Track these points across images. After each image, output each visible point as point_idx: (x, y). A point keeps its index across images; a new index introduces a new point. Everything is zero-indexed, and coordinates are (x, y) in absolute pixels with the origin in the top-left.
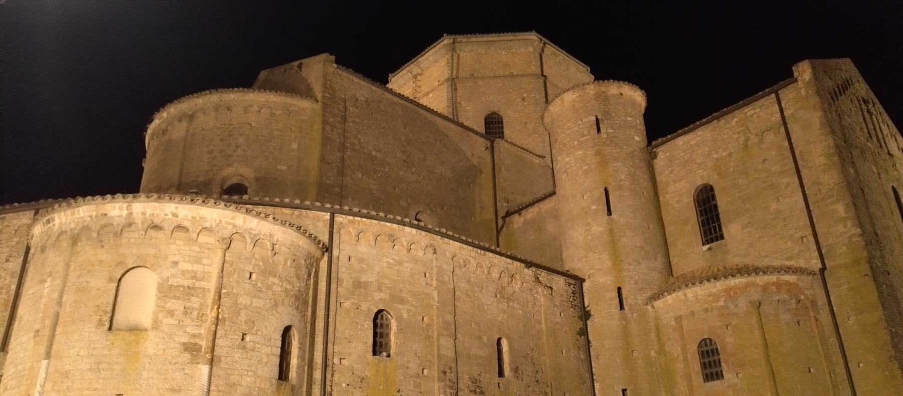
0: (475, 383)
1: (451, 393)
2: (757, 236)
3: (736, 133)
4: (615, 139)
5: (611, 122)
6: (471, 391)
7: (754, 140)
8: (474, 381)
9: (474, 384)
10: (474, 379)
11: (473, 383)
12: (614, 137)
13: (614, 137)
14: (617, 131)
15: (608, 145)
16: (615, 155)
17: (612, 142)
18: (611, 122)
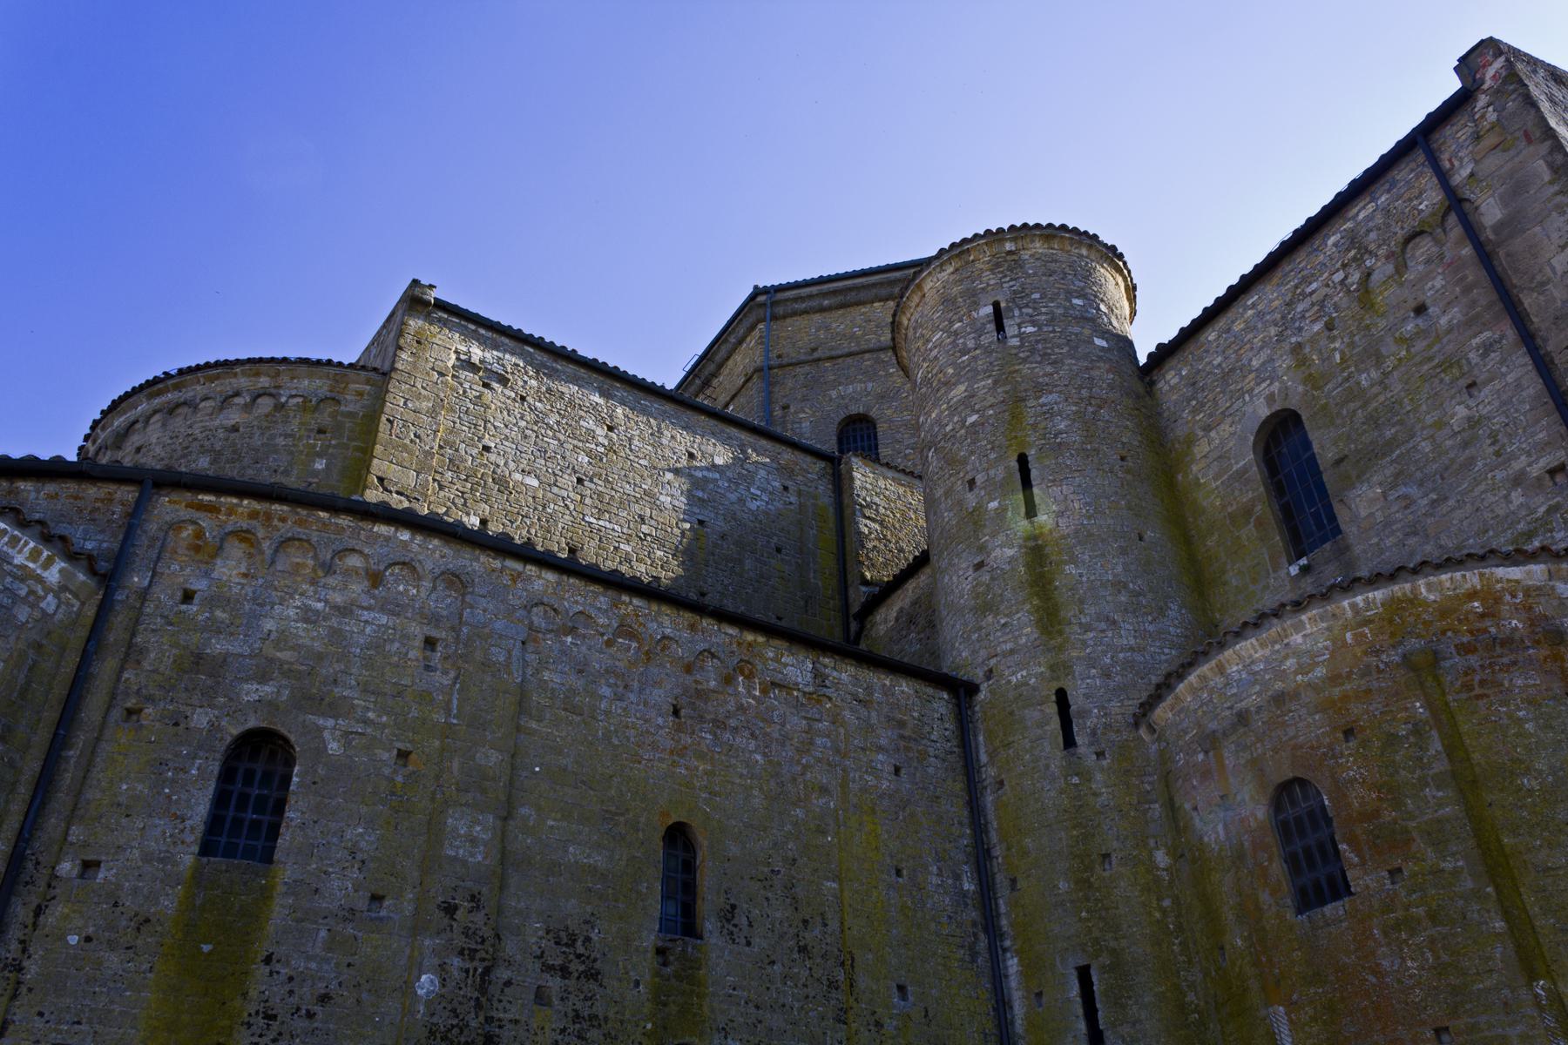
0: (567, 945)
1: (467, 971)
2: (1425, 501)
3: (1338, 270)
4: (1040, 346)
5: (1030, 311)
6: (548, 968)
7: (1382, 269)
8: (565, 940)
9: (564, 949)
10: (563, 934)
11: (557, 943)
12: (1037, 342)
13: (1037, 342)
14: (1045, 329)
15: (1025, 360)
16: (1041, 380)
17: (1033, 351)
18: (1030, 311)
